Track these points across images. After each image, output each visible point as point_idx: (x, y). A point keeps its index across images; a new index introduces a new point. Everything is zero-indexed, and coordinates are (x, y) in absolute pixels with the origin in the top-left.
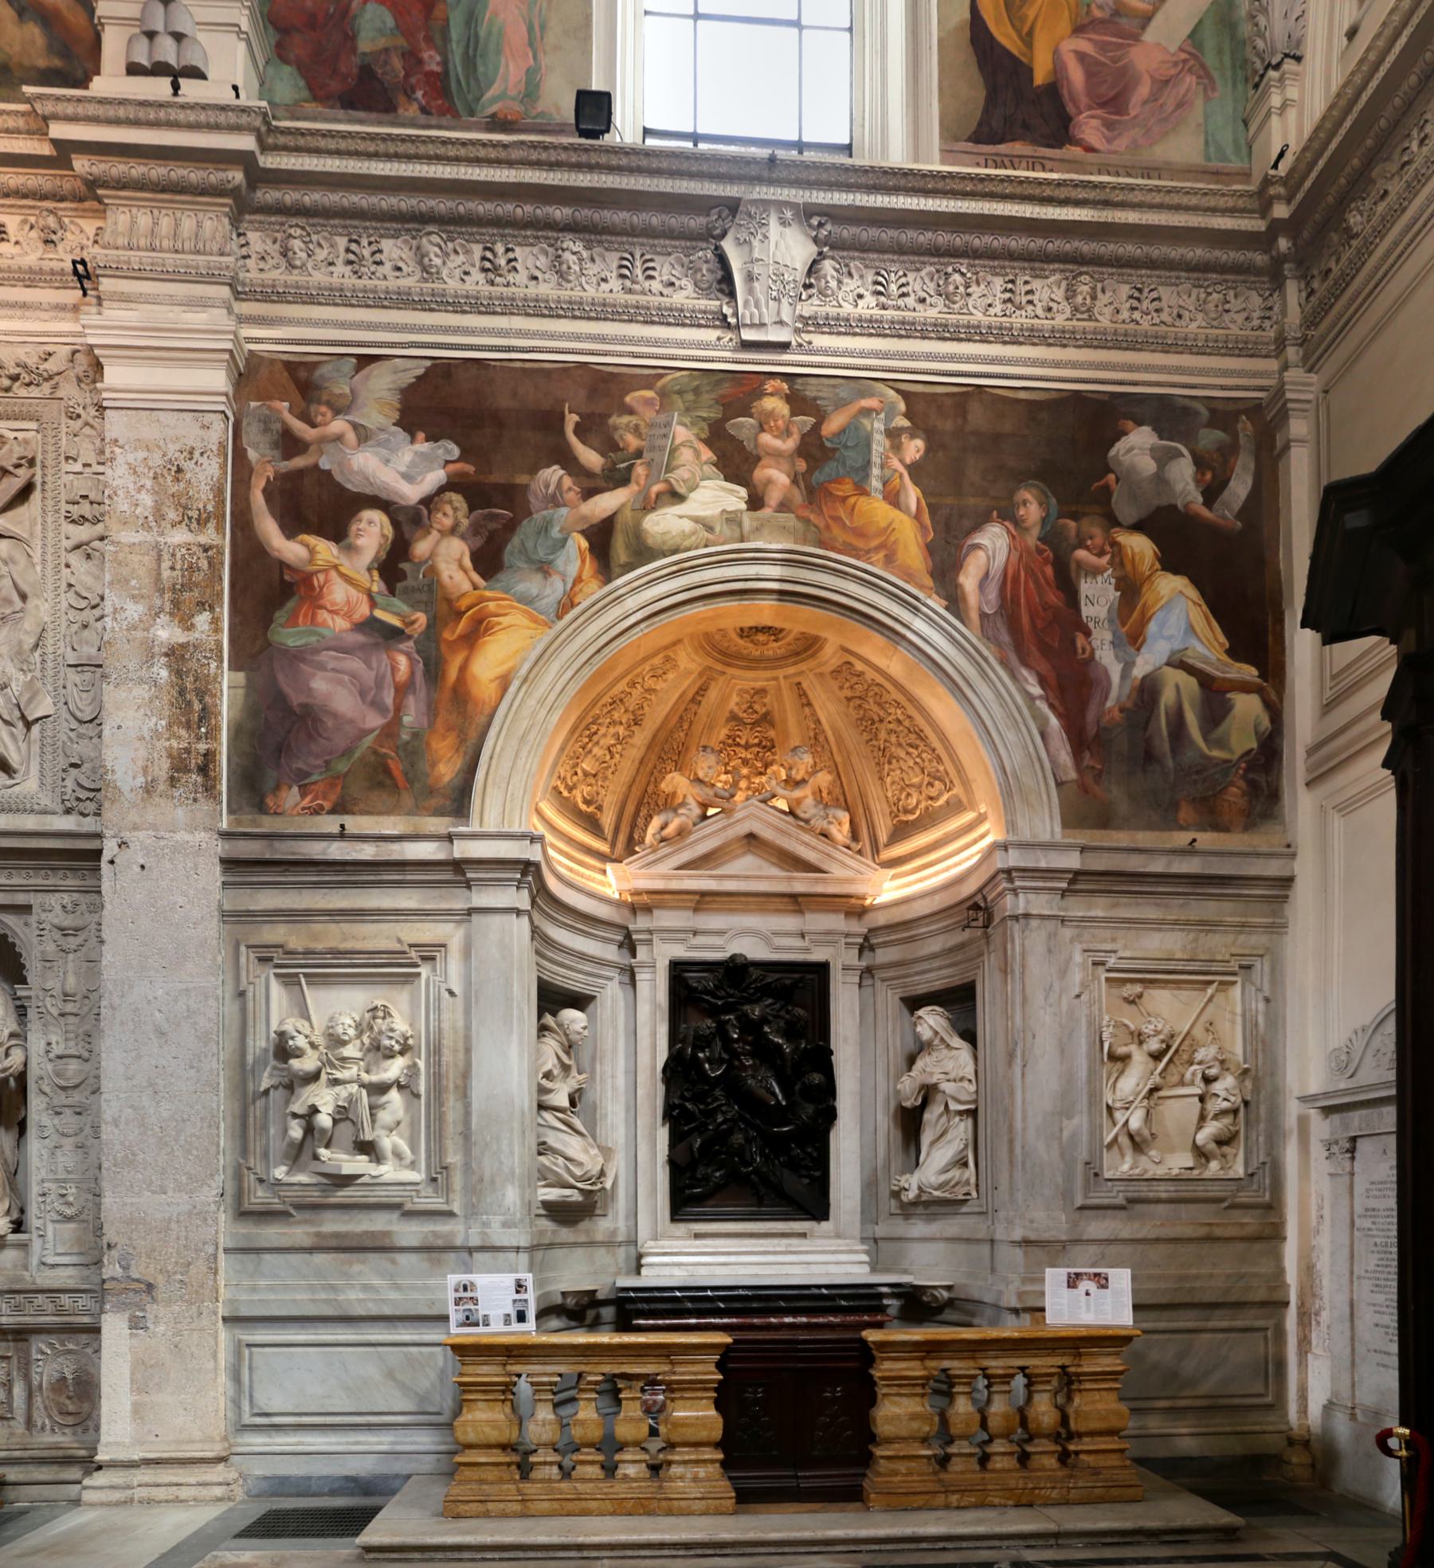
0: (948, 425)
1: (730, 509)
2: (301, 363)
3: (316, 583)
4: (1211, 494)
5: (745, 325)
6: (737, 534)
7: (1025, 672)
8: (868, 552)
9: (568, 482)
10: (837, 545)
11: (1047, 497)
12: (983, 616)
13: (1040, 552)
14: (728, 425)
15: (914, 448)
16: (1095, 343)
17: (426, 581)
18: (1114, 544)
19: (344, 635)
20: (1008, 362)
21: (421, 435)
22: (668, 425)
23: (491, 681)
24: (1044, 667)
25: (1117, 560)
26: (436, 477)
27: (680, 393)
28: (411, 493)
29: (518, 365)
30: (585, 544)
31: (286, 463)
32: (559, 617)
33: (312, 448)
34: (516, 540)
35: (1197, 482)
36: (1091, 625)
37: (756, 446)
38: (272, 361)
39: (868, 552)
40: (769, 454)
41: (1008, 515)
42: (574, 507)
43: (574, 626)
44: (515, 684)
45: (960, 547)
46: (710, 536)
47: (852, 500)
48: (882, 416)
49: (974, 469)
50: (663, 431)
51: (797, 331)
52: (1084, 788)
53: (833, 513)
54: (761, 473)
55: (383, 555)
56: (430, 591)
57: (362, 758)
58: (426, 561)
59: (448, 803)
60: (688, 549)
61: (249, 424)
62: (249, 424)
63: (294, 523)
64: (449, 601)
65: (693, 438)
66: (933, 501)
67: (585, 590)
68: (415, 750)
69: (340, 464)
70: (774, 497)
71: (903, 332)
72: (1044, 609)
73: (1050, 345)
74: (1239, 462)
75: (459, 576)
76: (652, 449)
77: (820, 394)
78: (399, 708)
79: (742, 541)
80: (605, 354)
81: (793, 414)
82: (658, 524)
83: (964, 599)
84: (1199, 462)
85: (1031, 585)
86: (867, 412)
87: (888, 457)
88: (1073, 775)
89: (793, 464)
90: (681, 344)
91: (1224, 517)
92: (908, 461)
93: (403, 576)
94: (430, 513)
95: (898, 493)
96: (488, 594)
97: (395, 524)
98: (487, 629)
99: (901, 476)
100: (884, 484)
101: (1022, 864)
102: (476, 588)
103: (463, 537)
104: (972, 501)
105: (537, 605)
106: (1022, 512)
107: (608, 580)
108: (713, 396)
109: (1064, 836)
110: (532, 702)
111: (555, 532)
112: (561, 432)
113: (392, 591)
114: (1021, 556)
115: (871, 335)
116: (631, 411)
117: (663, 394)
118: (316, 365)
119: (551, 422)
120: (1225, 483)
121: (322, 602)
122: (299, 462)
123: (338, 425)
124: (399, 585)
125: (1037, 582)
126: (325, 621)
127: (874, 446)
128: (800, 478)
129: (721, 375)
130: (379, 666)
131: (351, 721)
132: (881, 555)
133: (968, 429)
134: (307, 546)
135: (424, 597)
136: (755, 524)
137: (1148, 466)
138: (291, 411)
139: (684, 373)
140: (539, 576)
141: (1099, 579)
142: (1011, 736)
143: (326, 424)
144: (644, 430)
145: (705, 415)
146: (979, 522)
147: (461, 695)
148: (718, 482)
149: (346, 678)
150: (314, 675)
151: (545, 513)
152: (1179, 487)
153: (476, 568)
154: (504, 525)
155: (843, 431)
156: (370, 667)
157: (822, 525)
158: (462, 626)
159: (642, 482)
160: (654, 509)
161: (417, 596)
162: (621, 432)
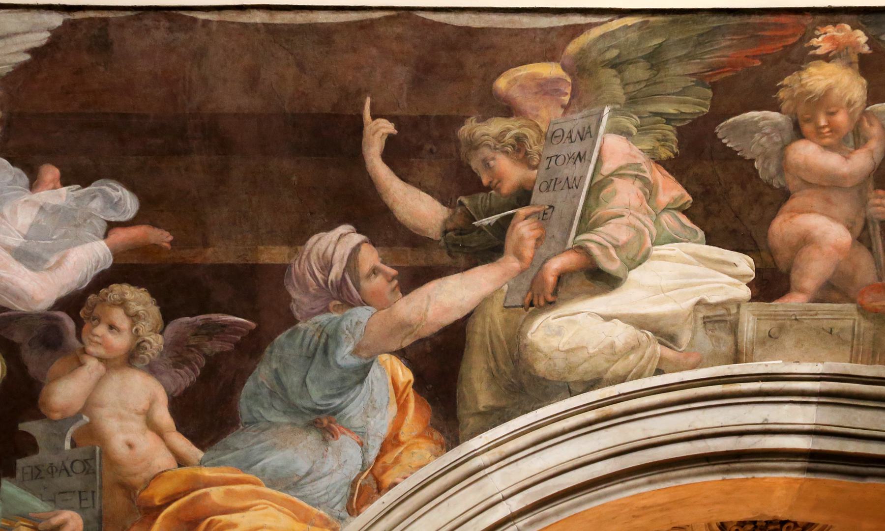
1: (713, 299)
6: (726, 347)
9: (370, 257)
14: (721, 130)
17: (78, 453)
21: (50, 173)
22: (588, 134)
27: (617, 65)
30: (405, 375)
34: (263, 373)
37: (782, 169)
40: (808, 185)
42: (389, 305)
46: (669, 353)
50: (577, 147)
56: (88, 468)
58: (78, 416)
60: (623, 379)
64: (128, 489)
65: (641, 159)
67: (406, 459)
75: (147, 443)
76: (551, 184)
79: (737, 360)
82: (559, 333)
89: (864, 203)
93: (30, 445)
96: (207, 472)
102: (181, 461)
103: (152, 370)
105: (308, 490)
107: (453, 440)
108: (693, 68)
111: (345, 355)
112: (357, 157)
116: (508, 110)
129: (715, 21)
135: (75, 482)
136: (766, 326)
139: (630, 21)
140: (312, 438)
144: (534, 147)
145: (670, 109)
148: (692, 247)
151: (323, 318)
153: (182, 426)
154: (238, 345)
159: (528, 253)
160: (550, 305)
161: (62, 481)
162: (486, 152)
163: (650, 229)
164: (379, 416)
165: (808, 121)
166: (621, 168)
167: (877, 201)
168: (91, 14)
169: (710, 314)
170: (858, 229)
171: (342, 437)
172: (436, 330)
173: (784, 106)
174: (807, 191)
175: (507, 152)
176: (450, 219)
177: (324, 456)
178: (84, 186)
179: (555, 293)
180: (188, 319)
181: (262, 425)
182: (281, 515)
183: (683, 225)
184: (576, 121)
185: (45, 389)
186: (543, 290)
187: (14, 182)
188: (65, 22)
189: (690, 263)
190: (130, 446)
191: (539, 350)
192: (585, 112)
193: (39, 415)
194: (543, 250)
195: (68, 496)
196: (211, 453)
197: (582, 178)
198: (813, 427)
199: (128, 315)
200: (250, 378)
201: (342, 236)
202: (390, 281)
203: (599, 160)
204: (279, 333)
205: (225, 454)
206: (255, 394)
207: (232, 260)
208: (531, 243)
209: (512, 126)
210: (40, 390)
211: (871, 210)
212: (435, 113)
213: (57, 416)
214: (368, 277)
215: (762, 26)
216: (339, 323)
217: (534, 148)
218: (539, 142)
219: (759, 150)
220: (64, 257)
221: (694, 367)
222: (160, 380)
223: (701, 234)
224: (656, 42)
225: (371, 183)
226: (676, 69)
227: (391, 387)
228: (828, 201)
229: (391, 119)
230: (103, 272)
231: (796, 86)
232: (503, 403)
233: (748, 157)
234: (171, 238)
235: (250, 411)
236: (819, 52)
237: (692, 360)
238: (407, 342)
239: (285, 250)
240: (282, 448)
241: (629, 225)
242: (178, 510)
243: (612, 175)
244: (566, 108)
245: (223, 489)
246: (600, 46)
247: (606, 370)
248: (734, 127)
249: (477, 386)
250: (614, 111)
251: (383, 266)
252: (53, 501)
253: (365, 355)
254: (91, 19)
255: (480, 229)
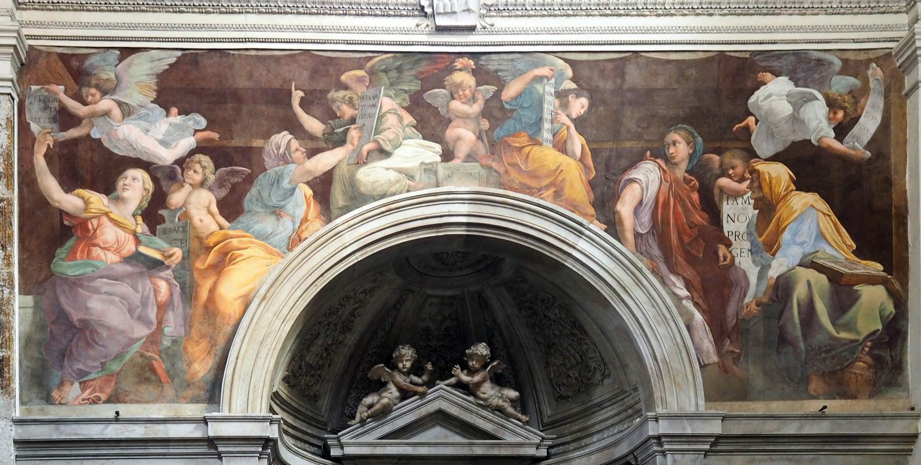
0: (609, 85)
1: (427, 161)
2: (73, 55)
3: (90, 226)
4: (841, 131)
5: (439, 14)
6: (433, 181)
7: (673, 278)
8: (540, 189)
9: (295, 144)
10: (514, 185)
11: (694, 137)
12: (637, 235)
13: (687, 181)
14: (425, 96)
15: (579, 106)
16: (739, 11)
17: (181, 224)
18: (753, 171)
19: (114, 266)
20: (662, 31)
21: (174, 110)
22: (376, 97)
23: (235, 299)
24: (690, 273)
25: (756, 184)
26: (188, 143)
27: (385, 71)
28: (167, 156)
29: (253, 53)
30: (310, 192)
31: (64, 133)
32: (290, 249)
33: (84, 122)
34: (254, 191)
35: (830, 120)
36: (732, 238)
37: (448, 111)
38: (49, 54)
39: (540, 189)
41: (660, 153)
42: (303, 163)
43: (302, 256)
44: (256, 302)
45: (617, 182)
46: (412, 183)
47: (527, 150)
48: (553, 81)
49: (630, 120)
50: (372, 102)
51: (482, 16)
52: (724, 369)
53: (511, 161)
54: (451, 133)
55: (145, 204)
56: (185, 231)
57: (132, 360)
58: (181, 208)
59: (202, 393)
60: (394, 194)
61: (31, 103)
62: (31, 103)
63: (70, 181)
64: (200, 239)
65: (396, 106)
66: (595, 146)
67: (310, 227)
68: (173, 355)
69: (108, 134)
70: (462, 151)
71: (571, 12)
72: (691, 228)
73: (698, 15)
74: (869, 102)
75: (208, 220)
76: (363, 116)
77: (501, 67)
78: (160, 323)
80: (324, 42)
81: (478, 84)
82: (369, 175)
83: (621, 223)
84: (832, 104)
85: (680, 210)
86: (540, 79)
87: (557, 114)
88: (714, 358)
90: (387, 31)
91: (854, 148)
92: (574, 116)
93: (162, 220)
94: (183, 171)
95: (565, 141)
96: (232, 232)
97: (155, 179)
98: (231, 260)
99: (568, 128)
100: (554, 136)
101: (671, 432)
102: (221, 228)
104: (628, 144)
105: (271, 240)
106: (672, 150)
107: (329, 220)
108: (413, 73)
109: (706, 409)
110: (269, 315)
111: (285, 184)
112: (290, 105)
113: (153, 232)
114: (670, 187)
115: (544, 16)
116: (346, 88)
117: (372, 73)
118: (86, 56)
119: (281, 97)
120: (856, 120)
121: (96, 241)
122: (73, 133)
123: (106, 104)
124: (158, 227)
125: (684, 206)
126: (98, 255)
127: (546, 106)
128: (484, 135)
129: (420, 56)
130: (144, 290)
131: (122, 332)
132: (551, 191)
133: (626, 86)
134: (83, 198)
135: (179, 236)
136: (447, 173)
137: (785, 109)
138: (66, 93)
140: (273, 218)
141: (740, 200)
142: (661, 330)
143: (96, 103)
144: (356, 102)
145: (406, 88)
146: (635, 160)
147: (211, 309)
149: (117, 299)
150: (90, 297)
151: (277, 169)
152: (813, 125)
153: (221, 213)
155: (520, 95)
156: (136, 291)
157: (502, 170)
158: (211, 258)
159: (356, 143)
160: (365, 163)
161: (174, 235)
162: (338, 103)
163: (401, 134)
164: (299, 209)
165: (456, 93)
166: (389, 110)
167: (483, 123)
168: (192, 51)
169: (427, 167)
170: (477, 134)
171: (284, 218)
172: (321, 174)
173: (447, 87)
174: (458, 119)
175: (346, 104)
176: (326, 129)
177: (278, 226)
178: (187, 115)
179: (367, 159)
180: (225, 168)
181: (253, 213)
182: (261, 251)
183: (414, 132)
184: (371, 92)
185: (169, 196)
186: (362, 158)
187: (160, 114)
188: (182, 54)
189: (417, 147)
190: (201, 221)
191: (361, 182)
192: (375, 89)
193: (166, 207)
194: (361, 141)
195: (176, 242)
196: (233, 224)
197: (375, 114)
198: (467, 213)
199: (201, 167)
200: (249, 193)
201: (284, 136)
202: (303, 153)
203: (381, 106)
204: (260, 174)
205: (238, 225)
206: (251, 200)
207: (242, 145)
208: (357, 139)
209: (348, 94)
210: (167, 197)
211: (482, 127)
212: (319, 88)
213: (173, 208)
214: (294, 152)
215: (436, 58)
216: (283, 171)
217: (357, 102)
218: (358, 100)
219: (440, 104)
220: (178, 143)
221: (421, 189)
222: (213, 194)
223: (421, 136)
224: (399, 63)
225: (295, 115)
226: (407, 73)
227: (304, 197)
228: (465, 123)
229: (302, 90)
230: (192, 149)
231: (450, 80)
232: (348, 204)
233: (436, 106)
234: (219, 136)
235: (248, 207)
236: (457, 68)
237: (421, 186)
238: (310, 179)
239: (262, 141)
240: (262, 222)
241: (393, 132)
242: (220, 248)
243: (386, 112)
244: (368, 87)
245: (237, 239)
246: (379, 64)
247: (388, 191)
248: (430, 95)
249: (338, 196)
250: (385, 88)
251: (300, 148)
252: (171, 244)
253: (293, 183)
254: (192, 53)
255: (337, 133)
